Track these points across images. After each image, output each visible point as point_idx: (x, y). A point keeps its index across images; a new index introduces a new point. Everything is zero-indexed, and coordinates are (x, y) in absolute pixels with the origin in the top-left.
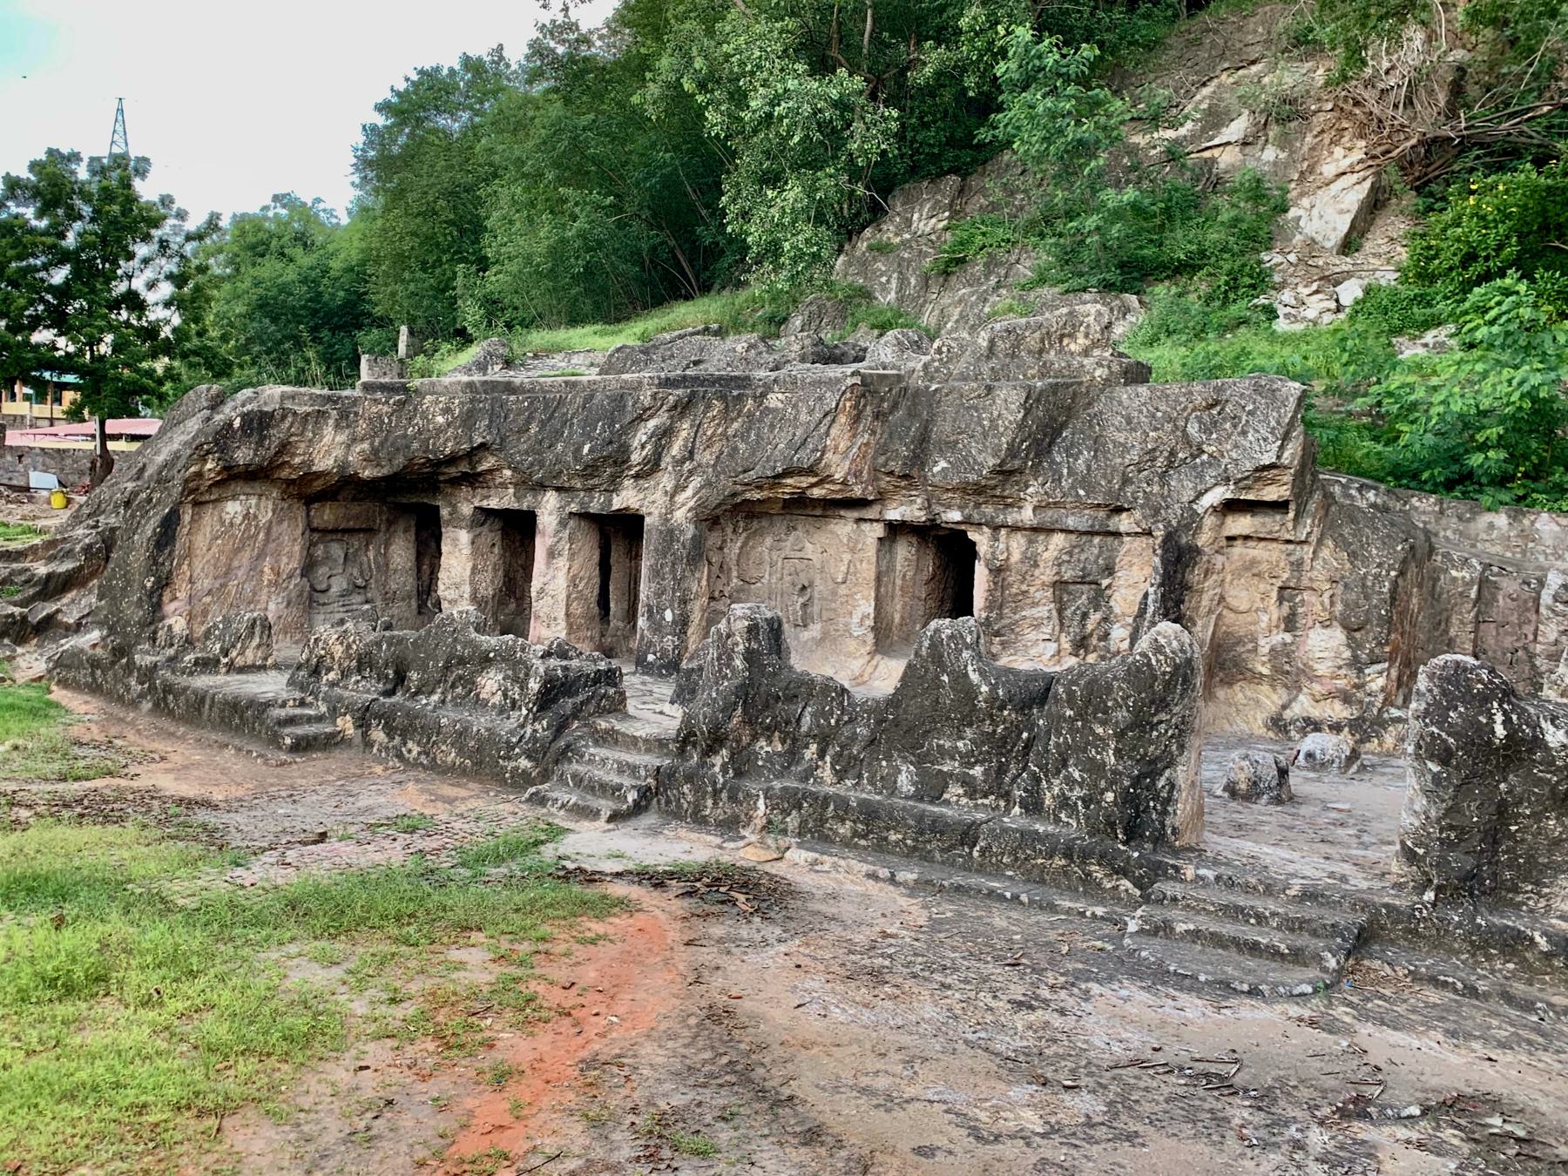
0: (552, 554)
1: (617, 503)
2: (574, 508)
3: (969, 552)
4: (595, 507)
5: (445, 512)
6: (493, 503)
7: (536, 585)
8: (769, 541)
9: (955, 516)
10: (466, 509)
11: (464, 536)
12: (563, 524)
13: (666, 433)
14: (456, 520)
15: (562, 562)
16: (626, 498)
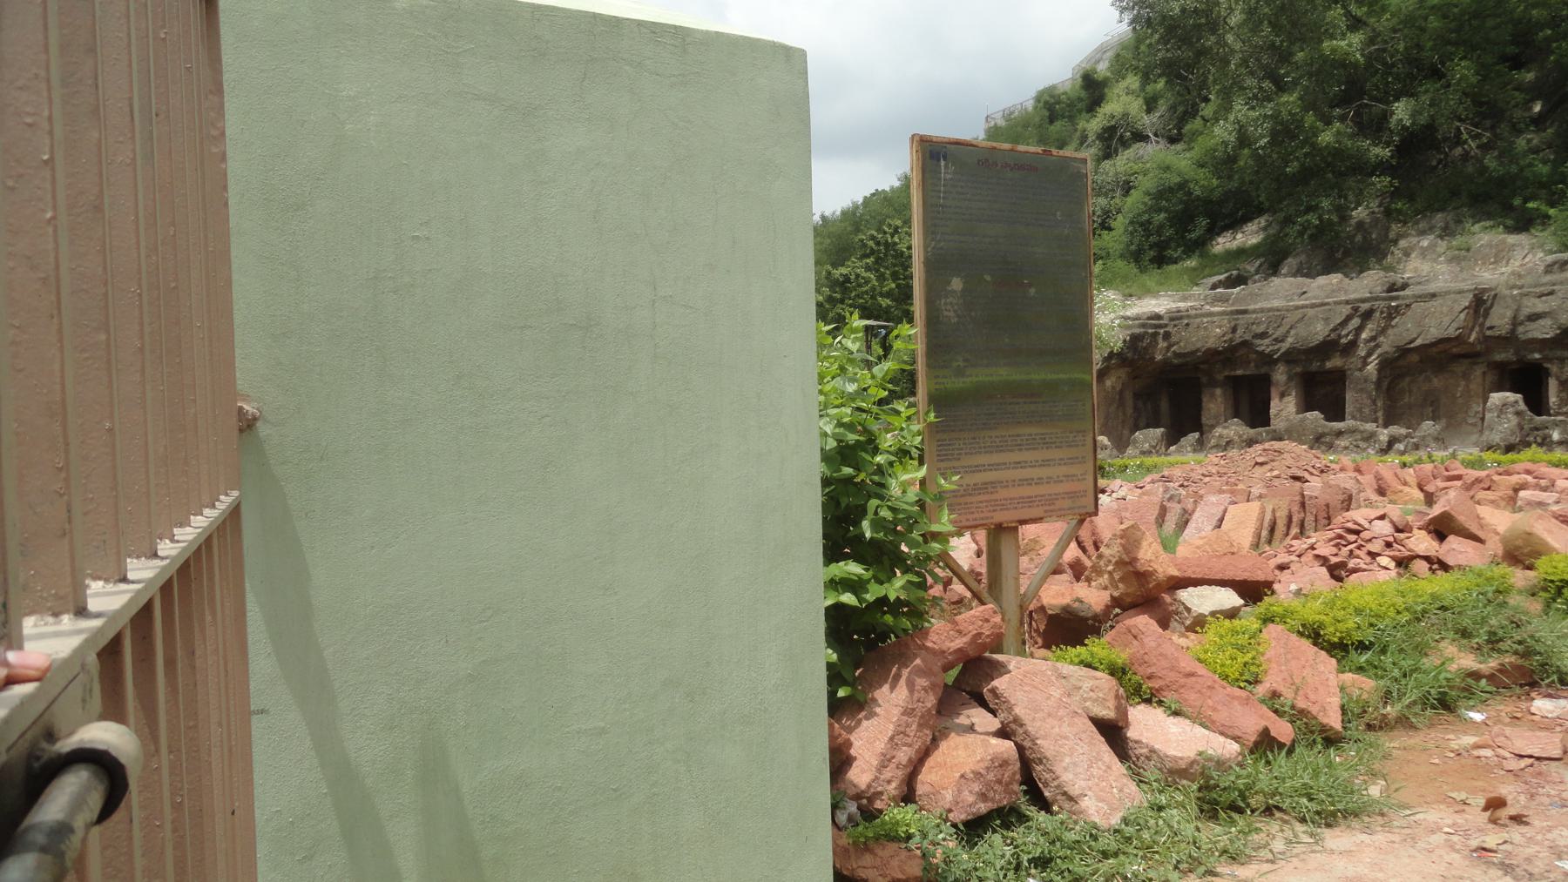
0: (1282, 395)
1: (1329, 365)
2: (1299, 369)
3: (1547, 373)
4: (1315, 366)
5: (1204, 380)
6: (1239, 372)
7: (1273, 411)
8: (1407, 379)
9: (1537, 356)
10: (1220, 377)
11: (1218, 391)
12: (1290, 379)
13: (1359, 330)
14: (1213, 384)
15: (1286, 399)
16: (1335, 362)
